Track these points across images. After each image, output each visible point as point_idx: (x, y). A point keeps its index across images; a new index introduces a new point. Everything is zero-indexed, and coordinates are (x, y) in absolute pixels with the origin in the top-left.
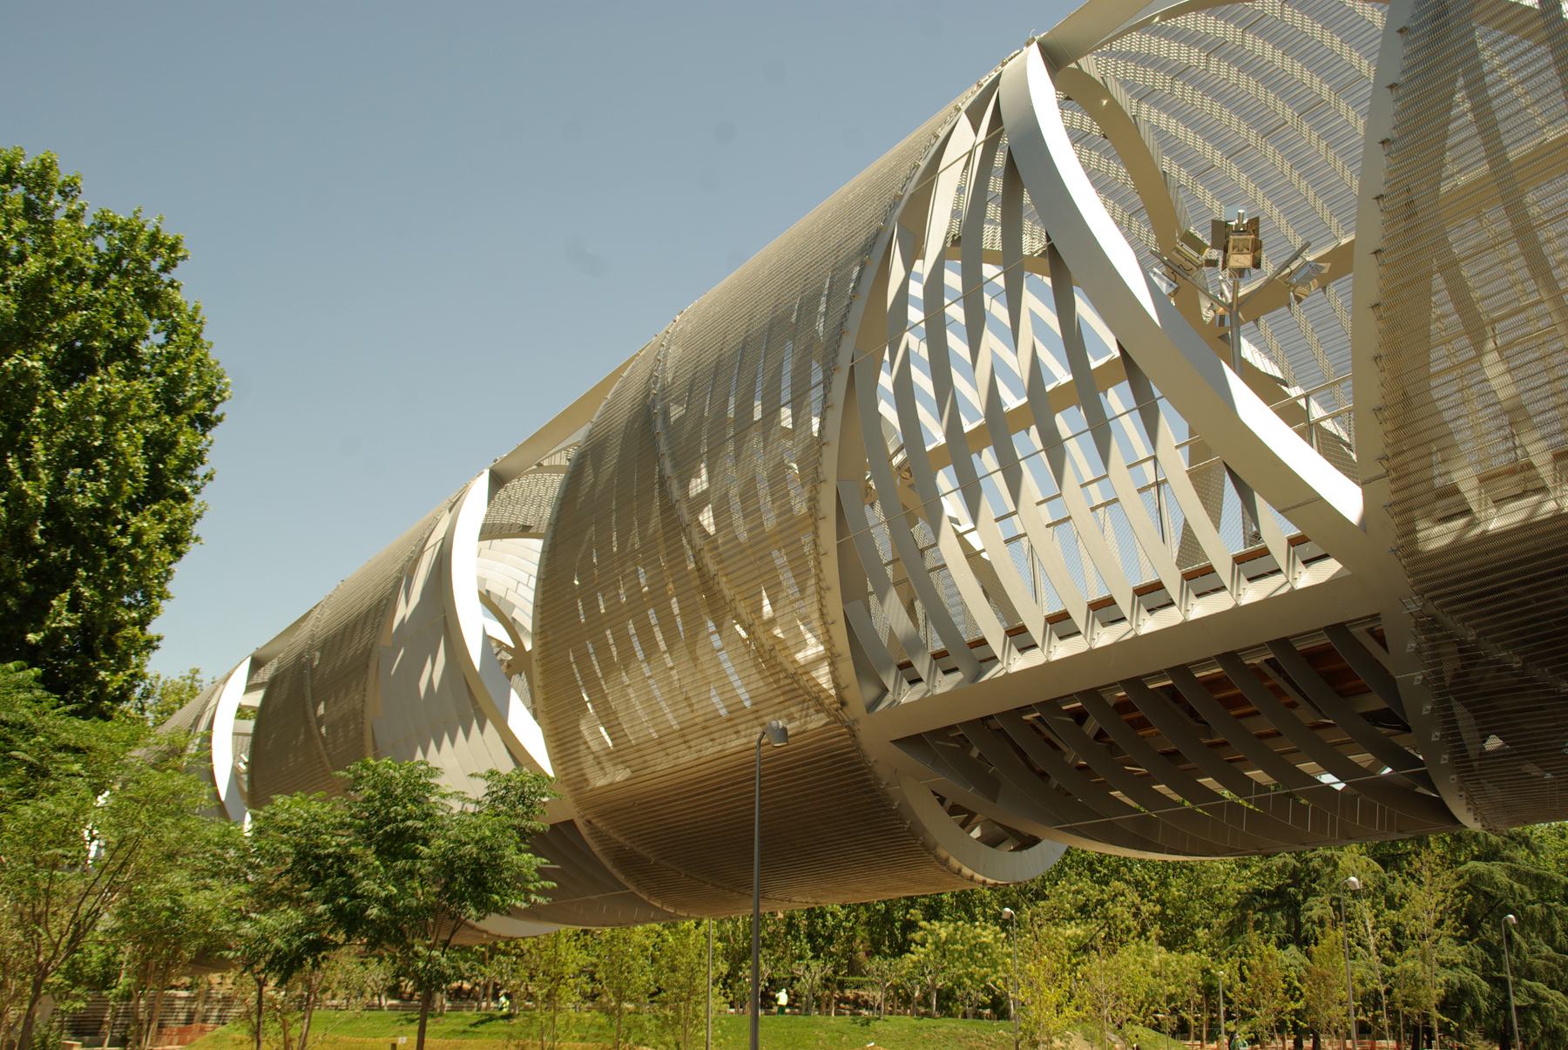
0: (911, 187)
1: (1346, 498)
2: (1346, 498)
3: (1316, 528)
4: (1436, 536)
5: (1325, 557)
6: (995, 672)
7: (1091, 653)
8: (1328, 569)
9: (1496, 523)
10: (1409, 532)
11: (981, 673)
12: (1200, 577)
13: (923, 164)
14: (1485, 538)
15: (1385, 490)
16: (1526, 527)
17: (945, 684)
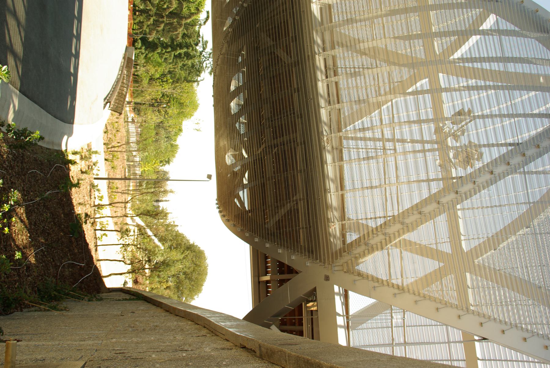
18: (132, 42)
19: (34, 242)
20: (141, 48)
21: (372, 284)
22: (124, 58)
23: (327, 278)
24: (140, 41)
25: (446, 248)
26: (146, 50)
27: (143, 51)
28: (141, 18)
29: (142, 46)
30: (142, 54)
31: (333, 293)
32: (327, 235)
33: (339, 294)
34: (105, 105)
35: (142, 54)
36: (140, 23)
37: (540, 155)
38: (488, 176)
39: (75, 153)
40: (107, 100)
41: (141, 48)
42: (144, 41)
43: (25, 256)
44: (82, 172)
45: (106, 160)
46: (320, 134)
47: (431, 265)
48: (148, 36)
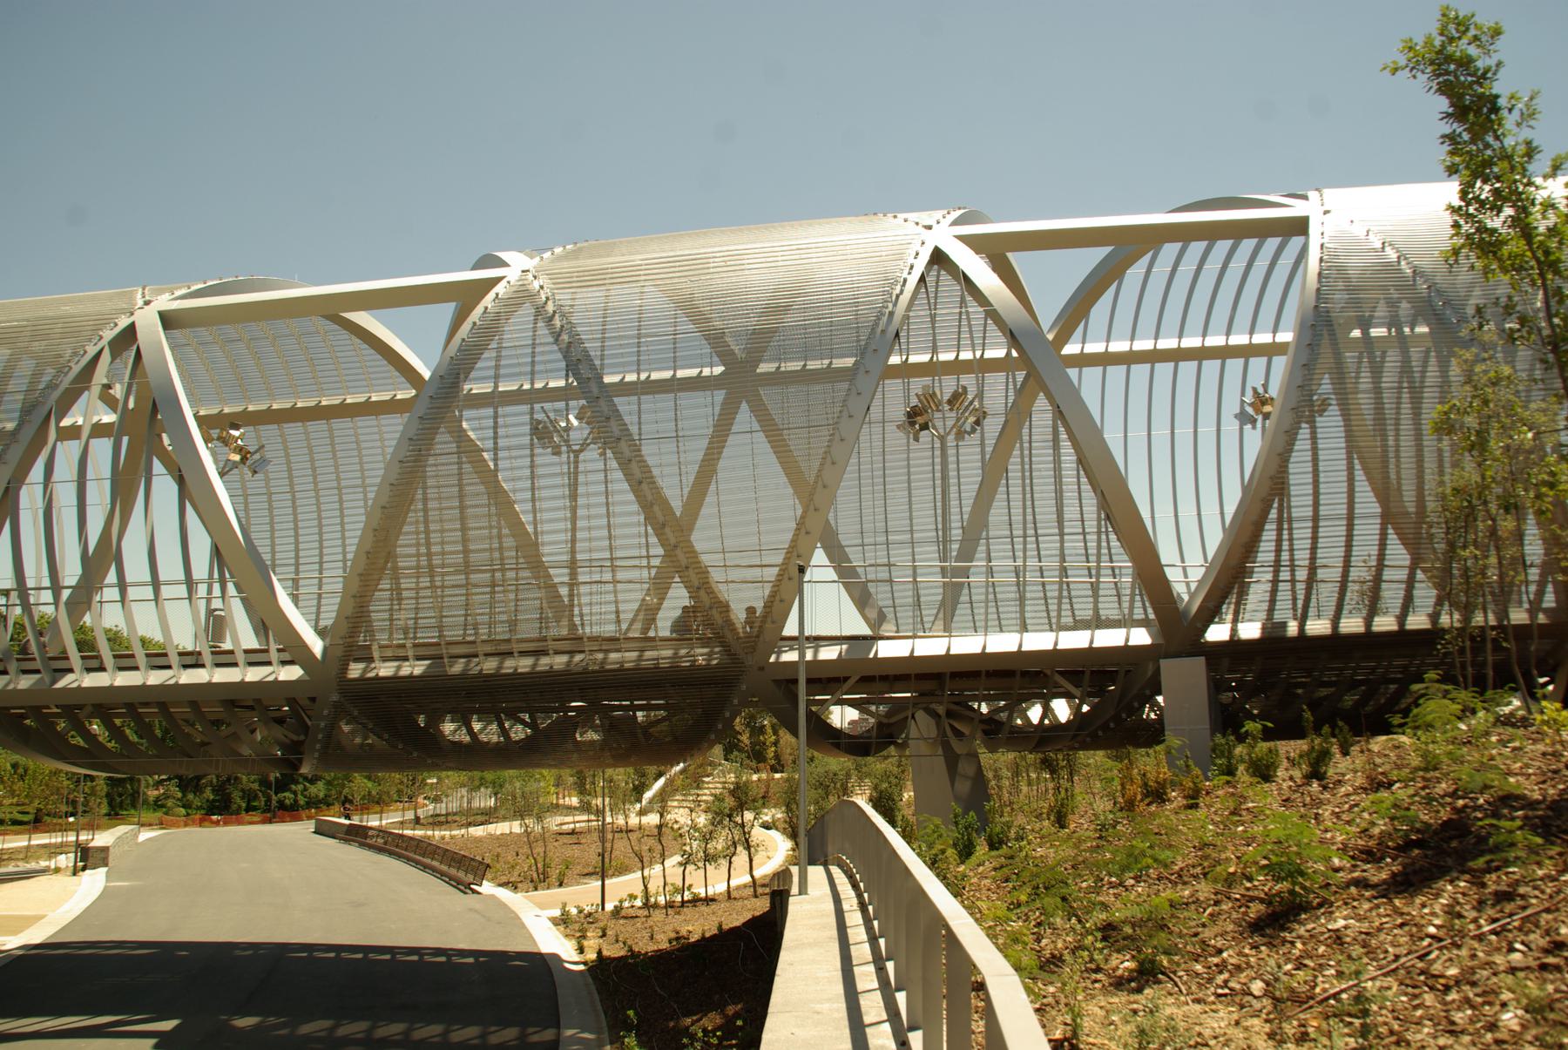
0: (66, 382)
1: (317, 646)
2: (317, 646)
3: (294, 651)
4: (355, 670)
5: (291, 662)
6: (65, 682)
7: (144, 686)
8: (293, 673)
9: (385, 670)
10: (345, 669)
11: (55, 681)
12: (225, 659)
13: (76, 369)
14: (377, 678)
15: (339, 652)
16: (394, 679)
17: (25, 682)
18: (288, 812)
19: (720, 1007)
20: (295, 793)
21: (768, 625)
22: (346, 841)
23: (762, 669)
24: (281, 795)
25: (720, 396)
26: (297, 783)
27: (300, 787)
28: (236, 796)
29: (290, 790)
30: (305, 789)
31: (777, 663)
32: (708, 667)
33: (779, 653)
34: (474, 892)
35: (305, 789)
36: (249, 796)
37: (619, 417)
38: (644, 486)
39: (581, 950)
40: (465, 888)
41: (295, 793)
42: (282, 786)
43: (737, 1015)
44: (604, 935)
45: (561, 885)
46: (585, 672)
47: (744, 416)
48: (272, 778)
